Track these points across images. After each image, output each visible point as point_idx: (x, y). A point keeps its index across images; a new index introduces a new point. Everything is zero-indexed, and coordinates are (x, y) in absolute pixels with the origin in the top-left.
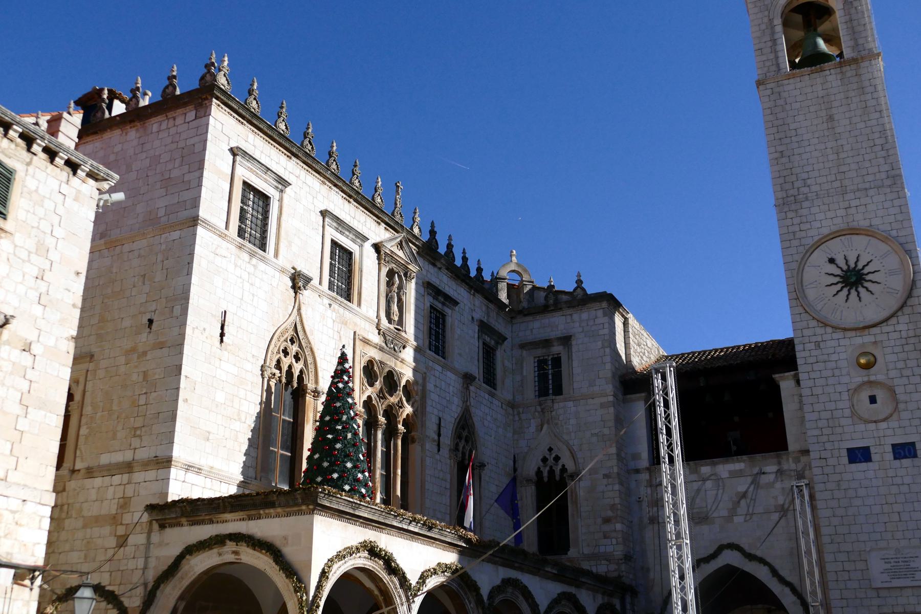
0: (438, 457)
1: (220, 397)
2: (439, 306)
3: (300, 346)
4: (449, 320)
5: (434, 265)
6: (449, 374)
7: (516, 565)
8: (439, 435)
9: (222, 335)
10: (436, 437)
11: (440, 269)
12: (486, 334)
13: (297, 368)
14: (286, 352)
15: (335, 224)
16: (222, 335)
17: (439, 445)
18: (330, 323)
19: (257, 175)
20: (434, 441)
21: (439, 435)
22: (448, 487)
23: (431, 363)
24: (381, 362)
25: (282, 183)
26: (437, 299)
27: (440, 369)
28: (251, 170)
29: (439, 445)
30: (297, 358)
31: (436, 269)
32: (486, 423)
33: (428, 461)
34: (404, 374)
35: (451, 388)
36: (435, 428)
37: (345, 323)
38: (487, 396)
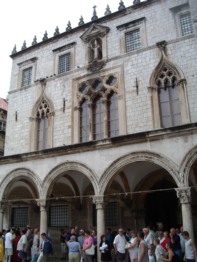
0: (138, 97)
1: (16, 136)
2: (132, 29)
3: (46, 102)
4: (141, 29)
5: (125, 15)
6: (144, 53)
7: (69, 152)
8: (137, 87)
9: (16, 118)
10: (135, 88)
11: (130, 13)
12: (180, 10)
13: (45, 110)
14: (41, 108)
15: (58, 51)
16: (16, 118)
17: (137, 91)
18: (59, 85)
19: (26, 65)
20: (133, 91)
21: (137, 87)
22: (149, 106)
23: (127, 58)
24: (88, 81)
25: (34, 60)
26: (129, 28)
27: (136, 55)
28: (24, 66)
29: (137, 91)
30: (45, 107)
31: (127, 16)
32: (187, 55)
33: (129, 103)
34: (104, 76)
35: (147, 58)
36: (135, 84)
37: (67, 80)
38: (187, 41)
